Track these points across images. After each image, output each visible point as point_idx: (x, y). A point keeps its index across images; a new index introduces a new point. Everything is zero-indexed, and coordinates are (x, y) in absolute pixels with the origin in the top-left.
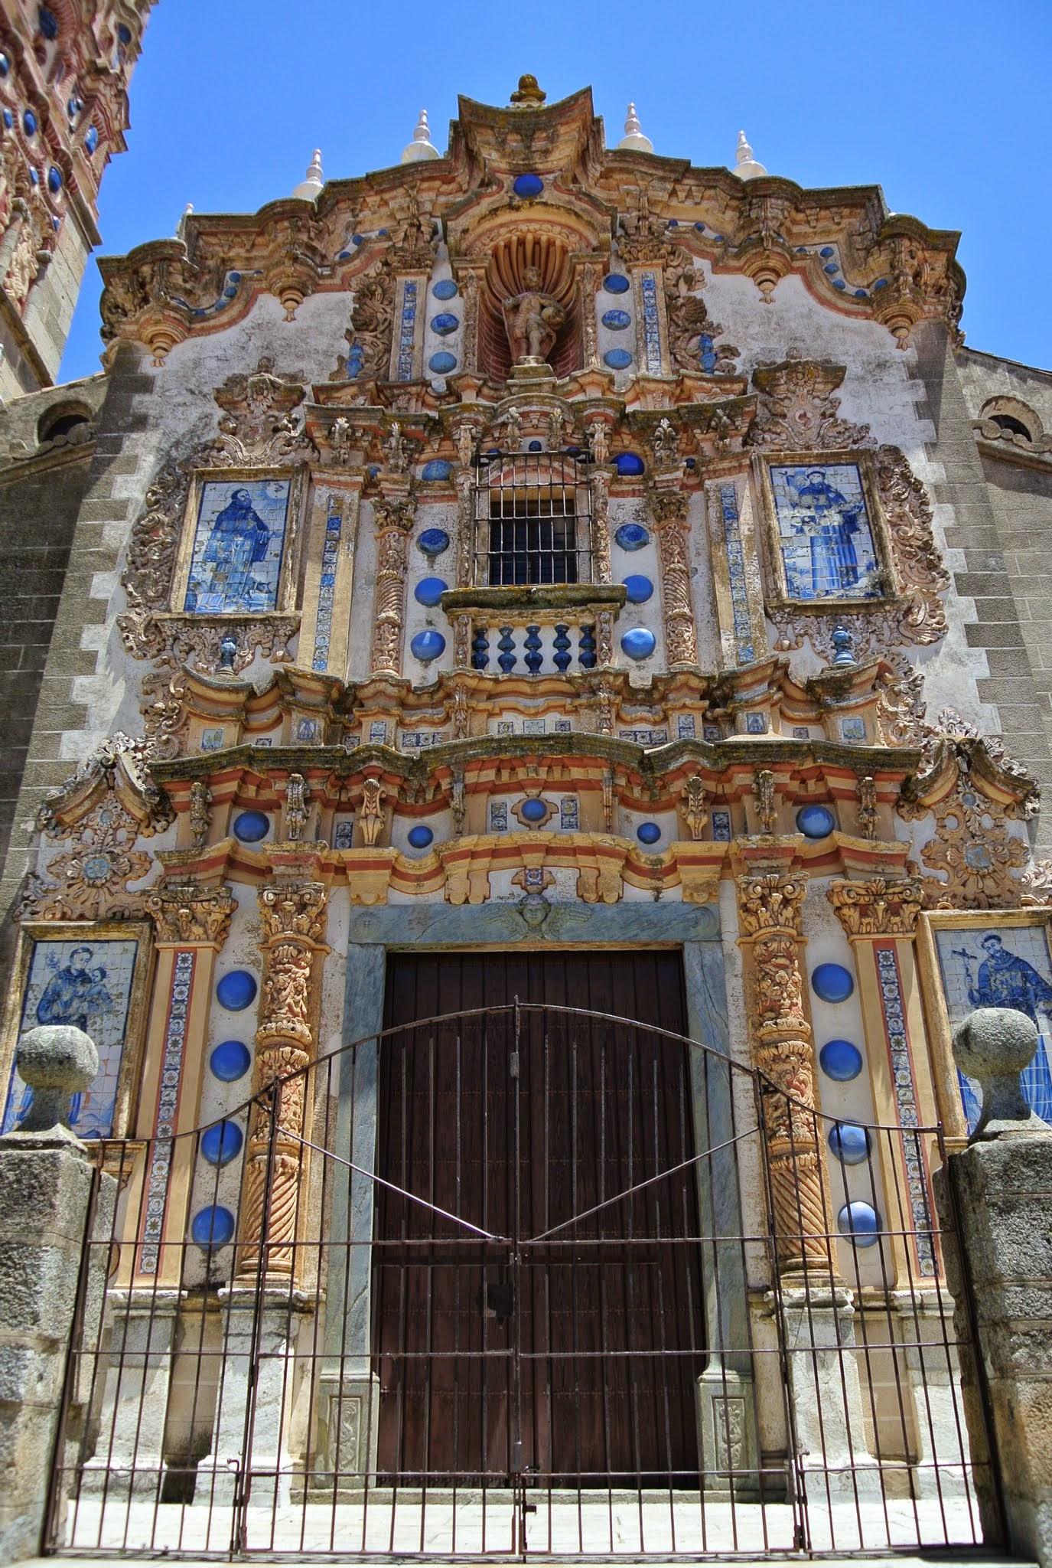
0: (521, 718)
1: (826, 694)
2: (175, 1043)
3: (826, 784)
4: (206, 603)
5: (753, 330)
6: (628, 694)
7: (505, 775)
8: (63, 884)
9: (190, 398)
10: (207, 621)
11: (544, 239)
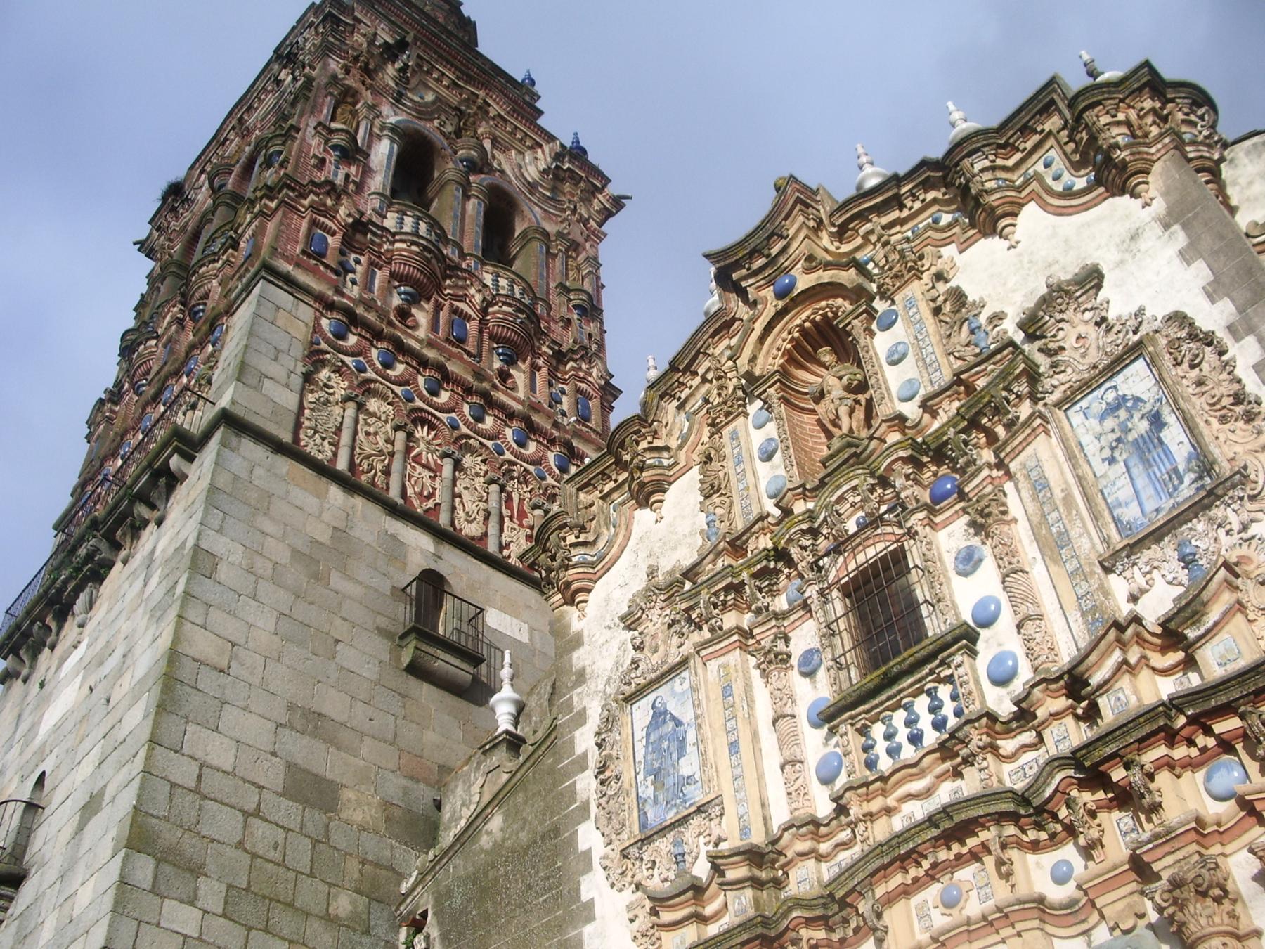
1: (1175, 635)
4: (656, 816)
5: (1010, 284)
9: (608, 633)
10: (656, 833)
11: (818, 318)
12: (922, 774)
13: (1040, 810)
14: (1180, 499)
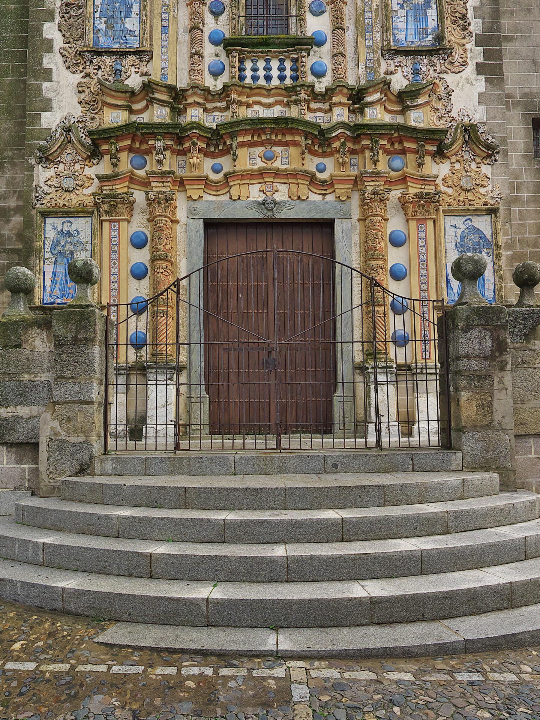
0: (262, 108)
1: (405, 99)
2: (115, 263)
3: (403, 144)
4: (104, 42)
6: (315, 96)
7: (256, 138)
8: (53, 190)
12: (268, 96)
13: (327, 139)
14: (423, 44)
